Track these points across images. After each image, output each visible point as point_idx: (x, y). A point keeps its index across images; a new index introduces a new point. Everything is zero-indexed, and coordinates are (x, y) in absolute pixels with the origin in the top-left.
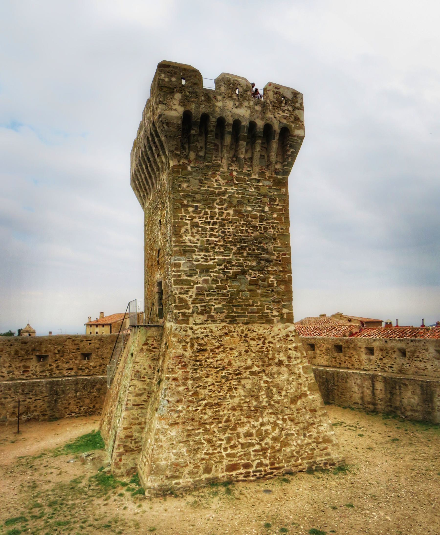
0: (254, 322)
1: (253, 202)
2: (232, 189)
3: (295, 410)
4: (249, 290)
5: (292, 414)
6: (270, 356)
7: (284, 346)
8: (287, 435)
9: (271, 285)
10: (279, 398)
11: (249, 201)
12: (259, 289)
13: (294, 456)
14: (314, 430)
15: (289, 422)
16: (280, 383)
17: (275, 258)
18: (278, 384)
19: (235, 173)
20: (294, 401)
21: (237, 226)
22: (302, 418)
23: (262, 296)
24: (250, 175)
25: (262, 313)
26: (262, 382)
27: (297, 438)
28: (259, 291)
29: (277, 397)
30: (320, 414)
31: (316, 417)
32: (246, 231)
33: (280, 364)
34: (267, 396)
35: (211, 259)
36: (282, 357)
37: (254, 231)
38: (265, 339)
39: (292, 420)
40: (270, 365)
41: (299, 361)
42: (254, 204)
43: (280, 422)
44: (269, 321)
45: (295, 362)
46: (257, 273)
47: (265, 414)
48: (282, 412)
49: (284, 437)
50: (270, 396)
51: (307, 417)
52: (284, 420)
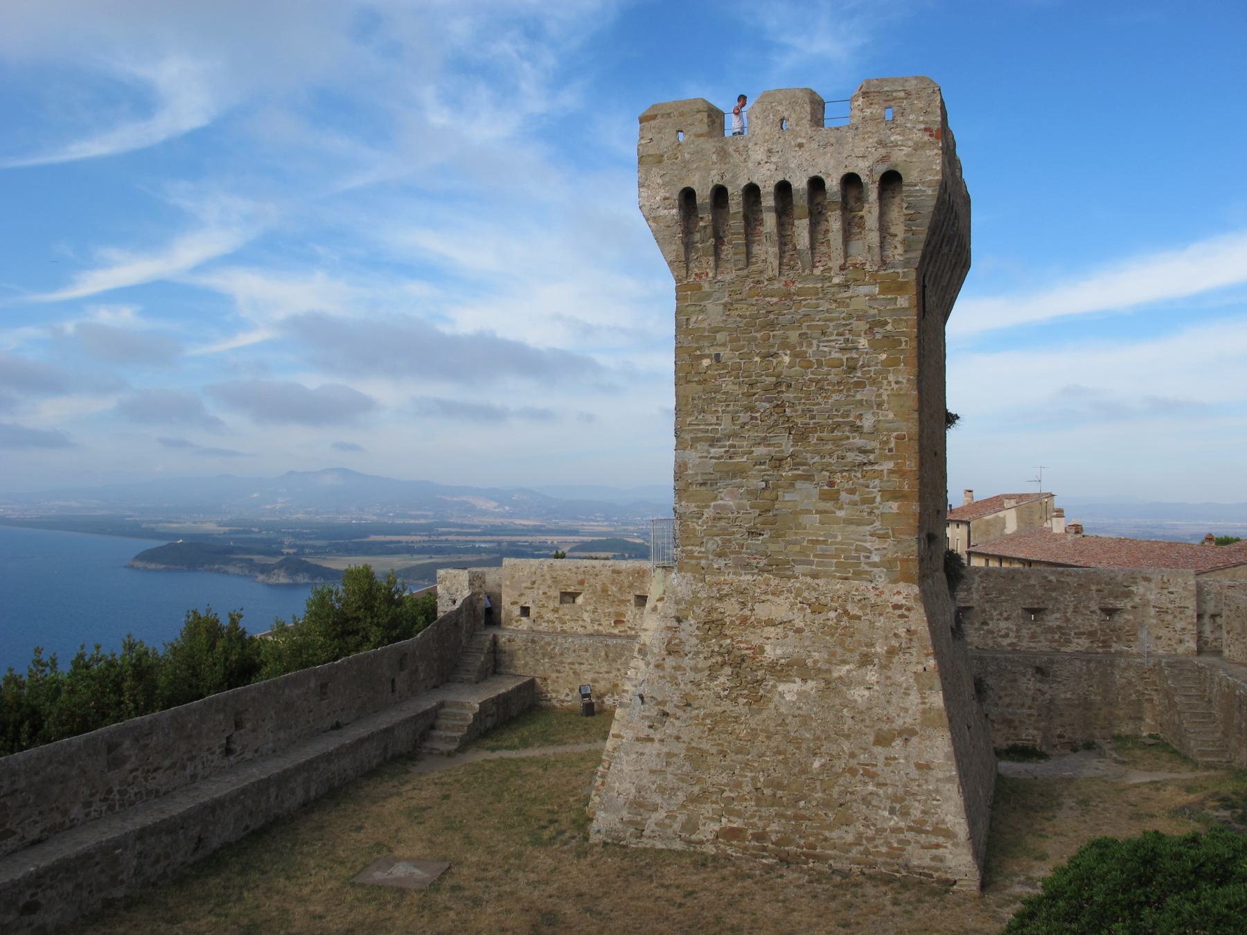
0: (828, 575)
1: (832, 334)
4: (817, 512)
11: (823, 333)
12: (841, 508)
14: (917, 804)
16: (860, 700)
18: (856, 701)
23: (848, 522)
24: (830, 279)
25: (846, 558)
28: (841, 514)
30: (940, 775)
31: (927, 781)
35: (744, 453)
42: (834, 338)
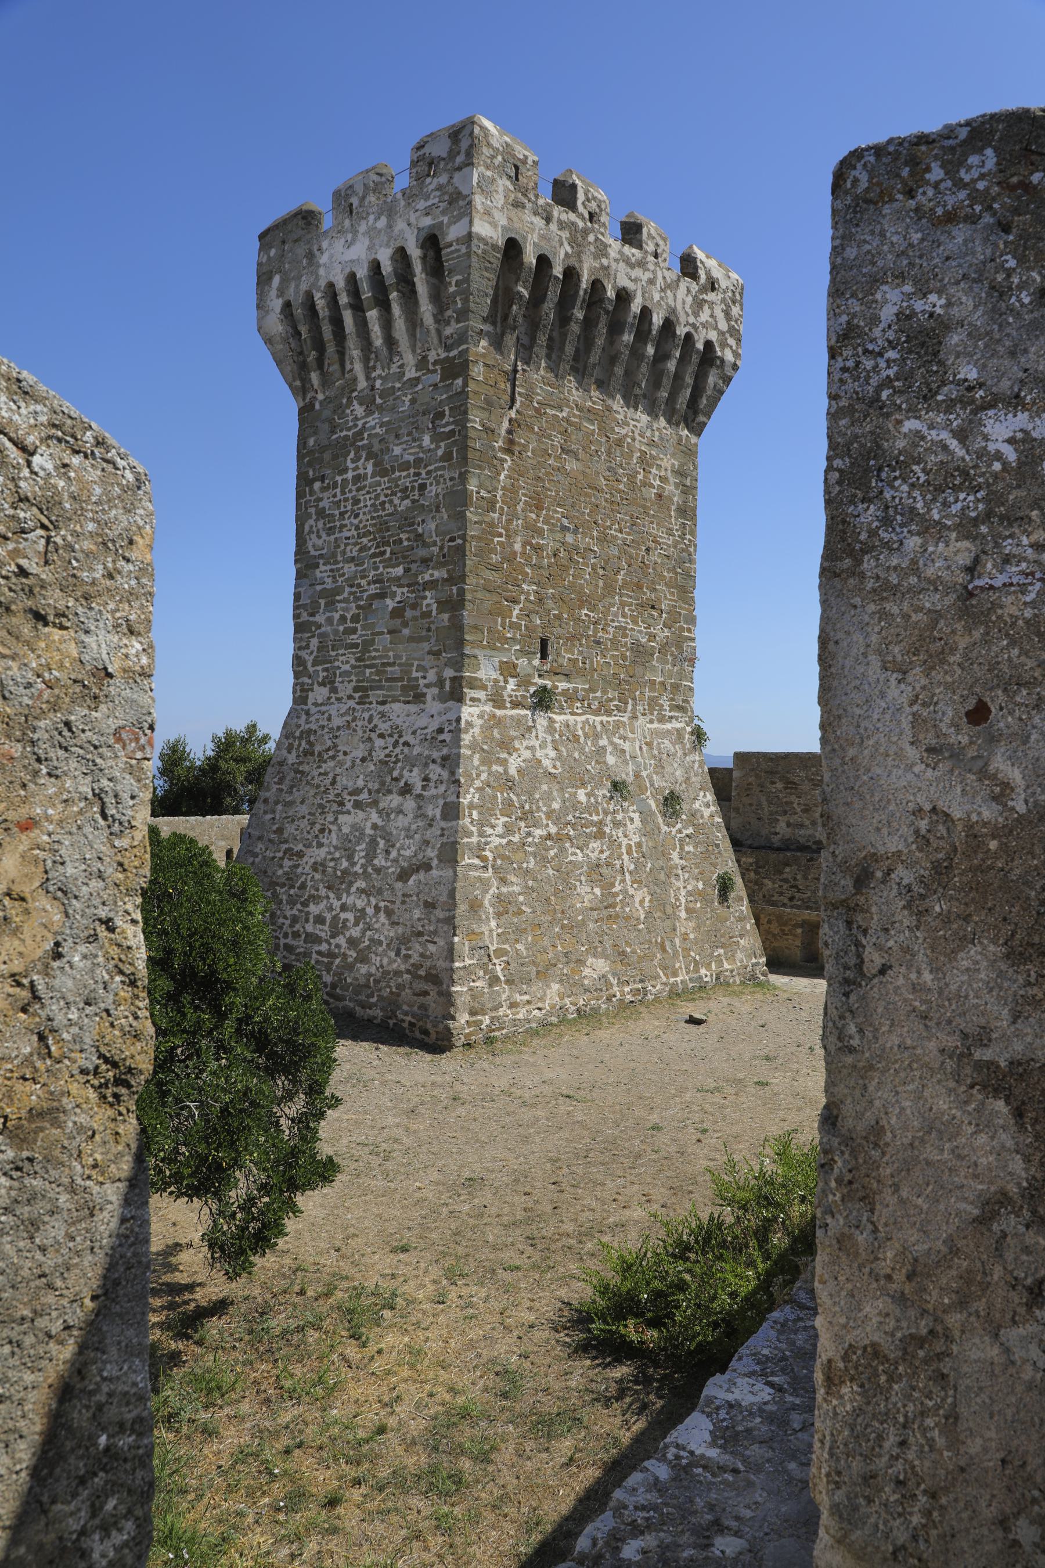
2: (372, 421)
3: (399, 894)
5: (393, 902)
6: (395, 774)
7: (426, 753)
8: (372, 940)
9: (427, 614)
10: (383, 863)
12: (405, 624)
13: (367, 986)
15: (382, 916)
17: (435, 550)
19: (378, 384)
20: (404, 876)
21: (377, 497)
22: (407, 916)
23: (411, 639)
26: (369, 824)
27: (384, 954)
29: (379, 861)
32: (391, 502)
33: (406, 790)
34: (367, 855)
36: (414, 777)
37: (403, 499)
38: (400, 736)
39: (389, 913)
40: (390, 792)
41: (442, 788)
43: (370, 911)
44: (419, 698)
45: (433, 792)
46: (405, 590)
47: (353, 889)
48: (380, 892)
49: (367, 943)
50: (370, 856)
51: (417, 913)
52: (377, 909)
